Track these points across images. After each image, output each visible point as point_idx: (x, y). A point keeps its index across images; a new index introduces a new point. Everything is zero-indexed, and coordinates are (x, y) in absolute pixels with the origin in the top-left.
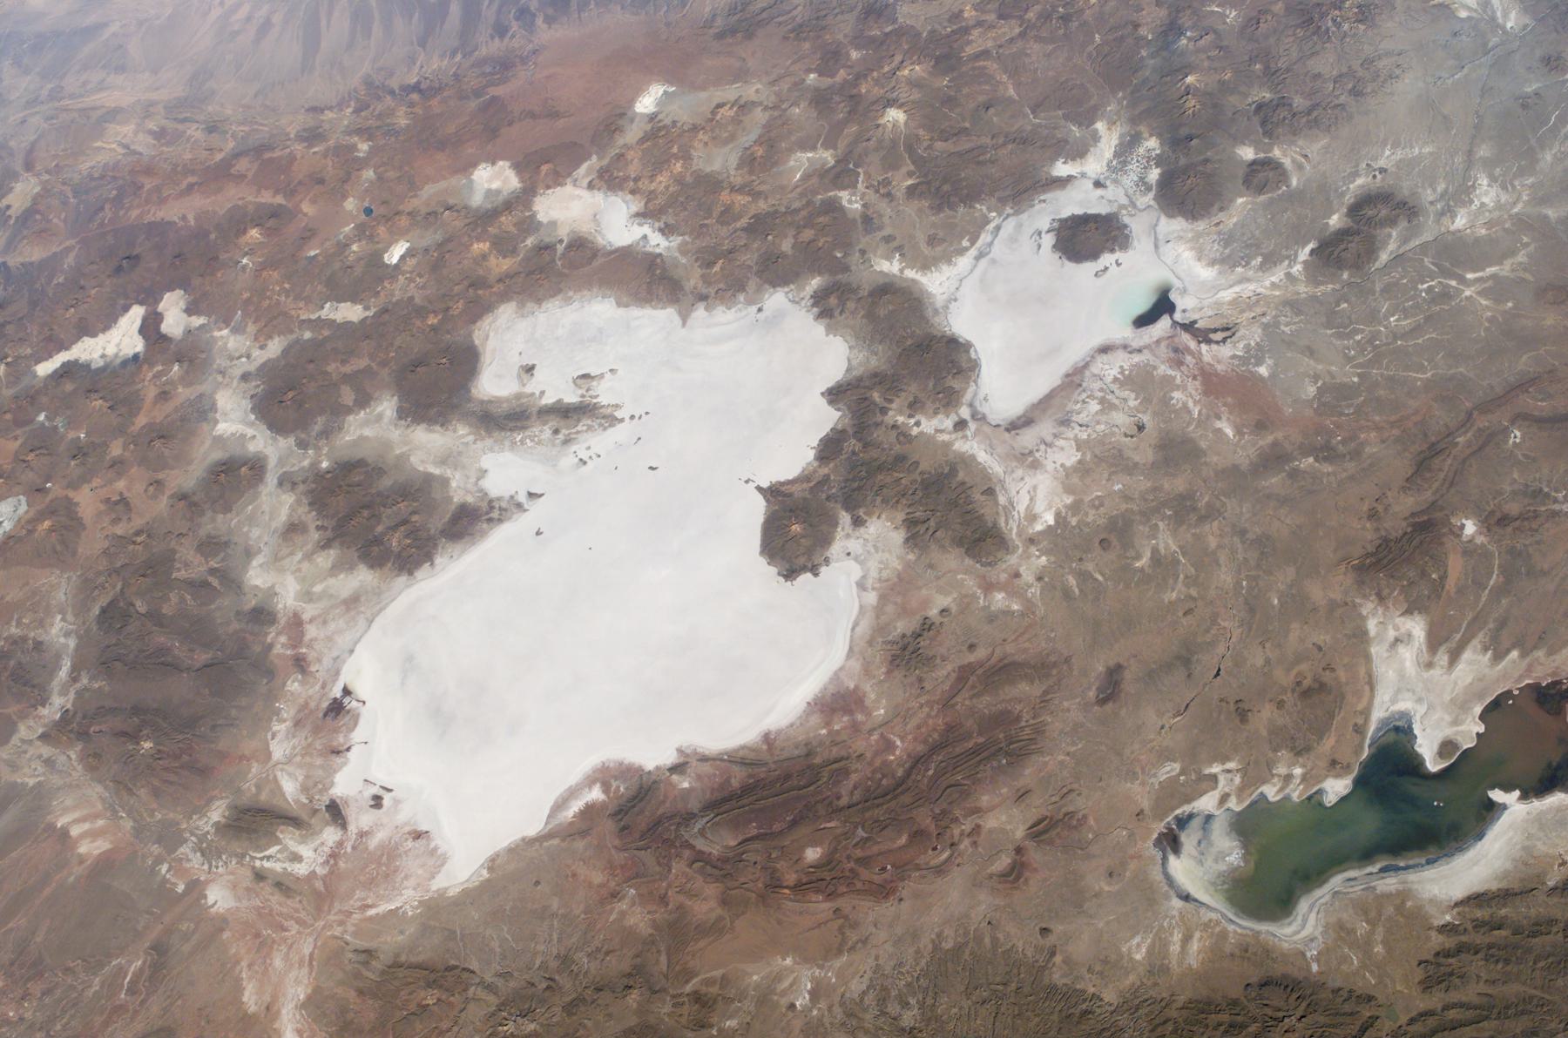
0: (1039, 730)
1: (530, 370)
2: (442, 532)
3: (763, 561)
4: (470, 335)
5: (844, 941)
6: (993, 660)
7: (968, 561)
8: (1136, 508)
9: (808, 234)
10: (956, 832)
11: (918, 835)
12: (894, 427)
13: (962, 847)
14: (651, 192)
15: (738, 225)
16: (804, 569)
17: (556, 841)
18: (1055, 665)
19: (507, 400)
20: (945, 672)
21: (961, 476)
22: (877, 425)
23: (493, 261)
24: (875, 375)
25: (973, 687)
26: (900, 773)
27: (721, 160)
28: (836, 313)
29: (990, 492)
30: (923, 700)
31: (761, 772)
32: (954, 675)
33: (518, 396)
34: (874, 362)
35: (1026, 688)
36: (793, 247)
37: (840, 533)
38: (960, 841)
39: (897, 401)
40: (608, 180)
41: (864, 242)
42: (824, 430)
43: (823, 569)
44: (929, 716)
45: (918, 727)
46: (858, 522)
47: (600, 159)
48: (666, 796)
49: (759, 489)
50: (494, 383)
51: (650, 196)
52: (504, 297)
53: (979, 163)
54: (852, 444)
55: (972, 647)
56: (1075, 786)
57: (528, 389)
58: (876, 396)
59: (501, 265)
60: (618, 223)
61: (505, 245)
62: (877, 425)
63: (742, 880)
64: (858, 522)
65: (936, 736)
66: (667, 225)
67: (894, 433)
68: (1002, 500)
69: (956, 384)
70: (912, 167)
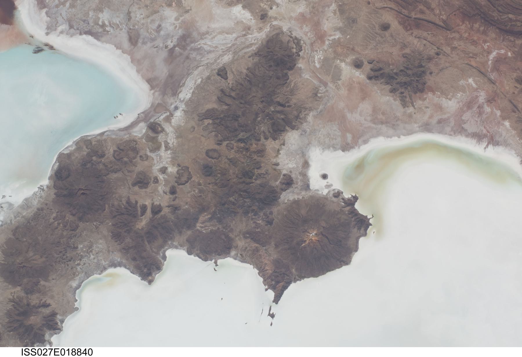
3: (356, 258)
7: (301, 64)
12: (173, 191)
16: (354, 213)
20: (416, 41)
21: (210, 106)
22: (175, 209)
24: (117, 236)
28: (46, 311)
29: (222, 73)
30: (447, 50)
32: (416, 32)
34: (101, 245)
37: (304, 194)
39: (141, 202)
42: (194, 259)
43: (347, 195)
44: (461, 38)
45: (474, 43)
46: (288, 182)
49: (277, 300)
54: (204, 225)
58: (142, 223)
62: (175, 209)
64: (288, 182)
67: (179, 188)
68: (227, 58)
69: (110, 150)
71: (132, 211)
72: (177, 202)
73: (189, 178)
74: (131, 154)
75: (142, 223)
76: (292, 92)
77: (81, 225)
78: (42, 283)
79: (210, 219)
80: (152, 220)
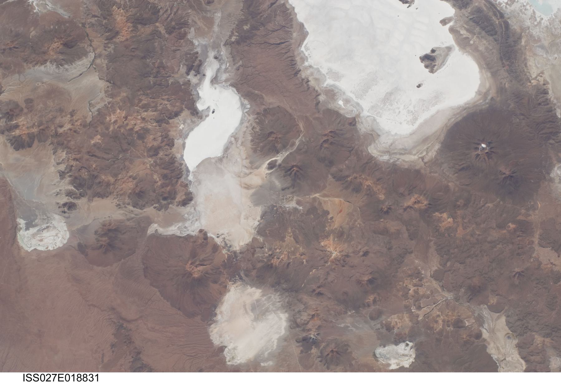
1: (430, 60)
4: (434, 162)
14: (159, 121)
19: (474, 51)
23: (338, 221)
27: (85, 81)
33: (463, 43)
40: (171, 185)
47: (149, 221)
50: (464, 82)
51: (166, 118)
52: (369, 165)
57: (449, 40)
59: (336, 206)
60: (216, 124)
66: (189, 69)
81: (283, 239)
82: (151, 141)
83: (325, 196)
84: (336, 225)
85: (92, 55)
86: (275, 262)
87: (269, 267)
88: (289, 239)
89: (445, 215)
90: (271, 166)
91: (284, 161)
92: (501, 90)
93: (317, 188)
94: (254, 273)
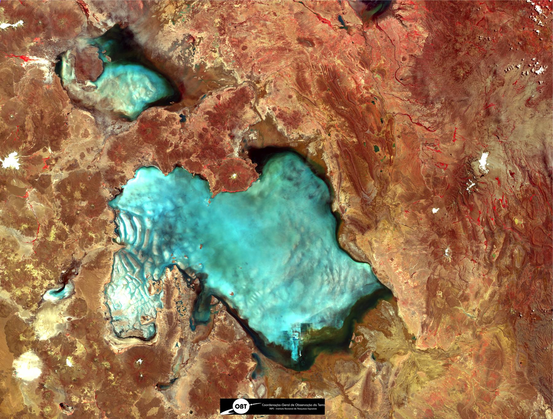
0: (325, 67)
2: (230, 341)
5: (410, 133)
6: (296, 89)
8: (228, 37)
9: (77, 194)
10: (367, 95)
11: (368, 109)
13: (372, 92)
14: (43, 278)
15: (67, 230)
17: (374, 255)
18: (298, 64)
21: (209, 110)
25: (307, 95)
26: (343, 119)
28: (122, 175)
30: (312, 114)
31: (344, 175)
32: (302, 103)
35: (307, 75)
36: (84, 201)
38: (370, 93)
41: (82, 167)
44: (319, 111)
48: (354, 213)
53: (42, 117)
55: (290, 97)
56: (347, 52)
58: (169, 151)
61: (69, 350)
63: (388, 175)
65: (327, 107)
70: (41, 150)
71: (166, 144)
72: (185, 146)
73: (193, 137)
74: (173, 120)
75: (169, 151)
76: (244, 113)
77: (145, 144)
78: (123, 163)
79: (197, 157)
80: (173, 150)
81: (56, 347)
82: (36, 283)
83: (79, 341)
84: (76, 354)
85: (36, 238)
86: (49, 353)
87: (46, 352)
88: (59, 348)
89: (113, 375)
90: (69, 319)
91: (74, 321)
92: (159, 345)
93: (79, 338)
94: (40, 351)
